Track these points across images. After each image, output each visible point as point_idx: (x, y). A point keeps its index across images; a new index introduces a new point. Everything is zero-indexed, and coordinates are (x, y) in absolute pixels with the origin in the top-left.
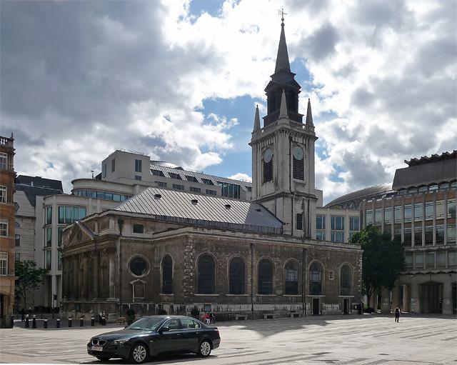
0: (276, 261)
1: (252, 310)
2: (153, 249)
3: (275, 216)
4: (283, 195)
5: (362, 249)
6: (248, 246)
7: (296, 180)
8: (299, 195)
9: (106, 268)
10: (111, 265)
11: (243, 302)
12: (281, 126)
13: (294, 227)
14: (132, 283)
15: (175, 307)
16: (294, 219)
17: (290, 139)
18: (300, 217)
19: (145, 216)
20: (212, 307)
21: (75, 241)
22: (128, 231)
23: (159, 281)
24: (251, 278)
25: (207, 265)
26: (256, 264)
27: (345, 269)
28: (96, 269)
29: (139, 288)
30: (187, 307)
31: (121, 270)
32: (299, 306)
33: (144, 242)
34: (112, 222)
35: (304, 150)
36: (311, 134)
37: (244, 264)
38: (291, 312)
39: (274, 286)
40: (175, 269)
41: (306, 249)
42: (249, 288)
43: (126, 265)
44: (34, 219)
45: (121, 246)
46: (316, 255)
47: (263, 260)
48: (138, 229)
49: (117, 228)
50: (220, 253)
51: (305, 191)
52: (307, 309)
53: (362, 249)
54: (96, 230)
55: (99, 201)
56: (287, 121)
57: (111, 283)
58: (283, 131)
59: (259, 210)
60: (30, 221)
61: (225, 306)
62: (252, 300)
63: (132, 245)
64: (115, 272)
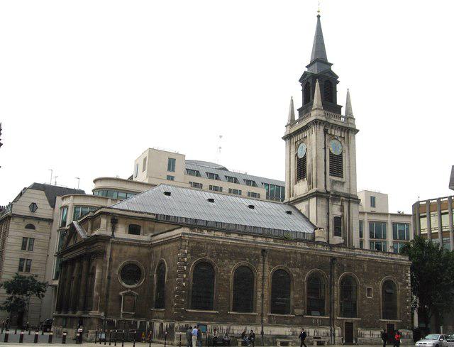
0: (295, 272)
1: (262, 333)
2: (149, 255)
3: (307, 220)
4: (317, 195)
5: (410, 260)
6: (259, 252)
8: (337, 197)
9: (93, 274)
10: (97, 271)
11: (251, 321)
12: (314, 118)
13: (331, 234)
14: (121, 293)
15: (165, 324)
16: (331, 223)
17: (326, 132)
18: (338, 221)
19: (143, 215)
20: (209, 327)
21: (72, 243)
22: (122, 233)
23: (152, 292)
24: (263, 292)
25: (204, 273)
26: (268, 274)
27: (388, 284)
29: (129, 300)
30: (176, 325)
31: (109, 277)
32: (323, 331)
33: (140, 246)
34: (104, 221)
35: (343, 144)
36: (350, 126)
37: (253, 276)
38: (315, 338)
39: (292, 303)
40: (168, 277)
42: (259, 305)
44: (51, 221)
45: (112, 250)
46: (349, 266)
47: (279, 270)
48: (134, 230)
49: (109, 228)
50: (222, 259)
51: (344, 190)
52: (337, 335)
53: (410, 260)
54: (89, 230)
55: (109, 200)
56: (322, 113)
57: (96, 293)
58: (316, 122)
59: (289, 213)
60: (46, 224)
61: (225, 327)
62: (262, 321)
63: (125, 248)
64: (102, 280)
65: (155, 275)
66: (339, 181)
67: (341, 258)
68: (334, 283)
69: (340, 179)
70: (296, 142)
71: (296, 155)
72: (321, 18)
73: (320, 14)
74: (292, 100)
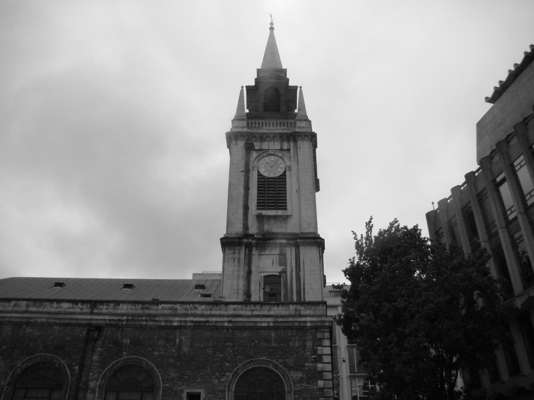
7: (264, 212)
17: (249, 148)
41: (99, 328)
51: (292, 227)
66: (275, 217)
67: (116, 326)
68: (87, 385)
69: (280, 212)
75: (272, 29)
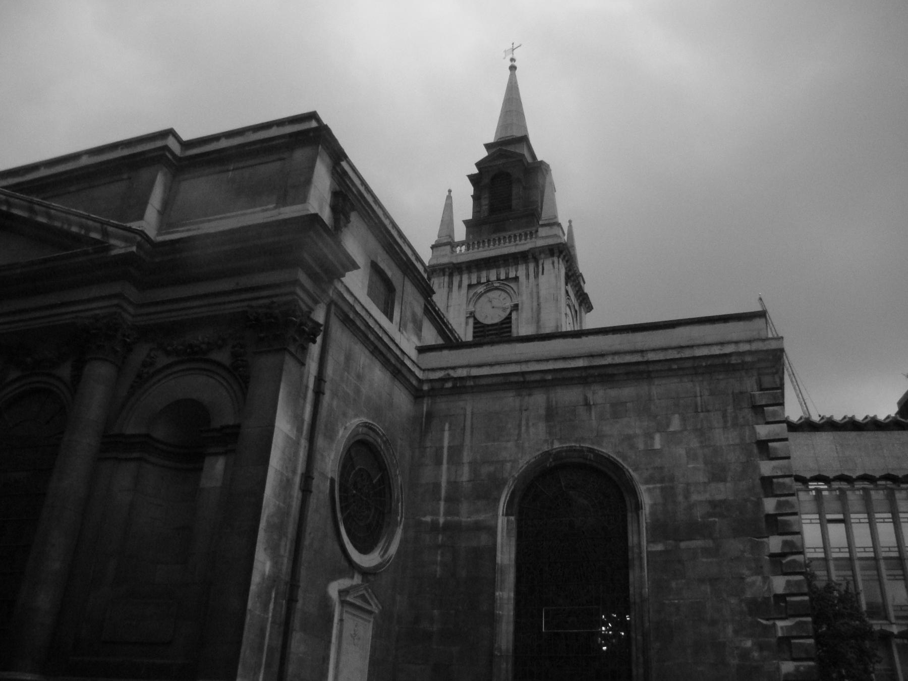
2: (424, 424)
28: (83, 443)
43: (330, 464)
63: (362, 357)
64: (285, 485)
65: (503, 523)
70: (470, 286)
71: (472, 315)
72: (517, 72)
73: (516, 64)
74: (449, 197)
75: (513, 68)
